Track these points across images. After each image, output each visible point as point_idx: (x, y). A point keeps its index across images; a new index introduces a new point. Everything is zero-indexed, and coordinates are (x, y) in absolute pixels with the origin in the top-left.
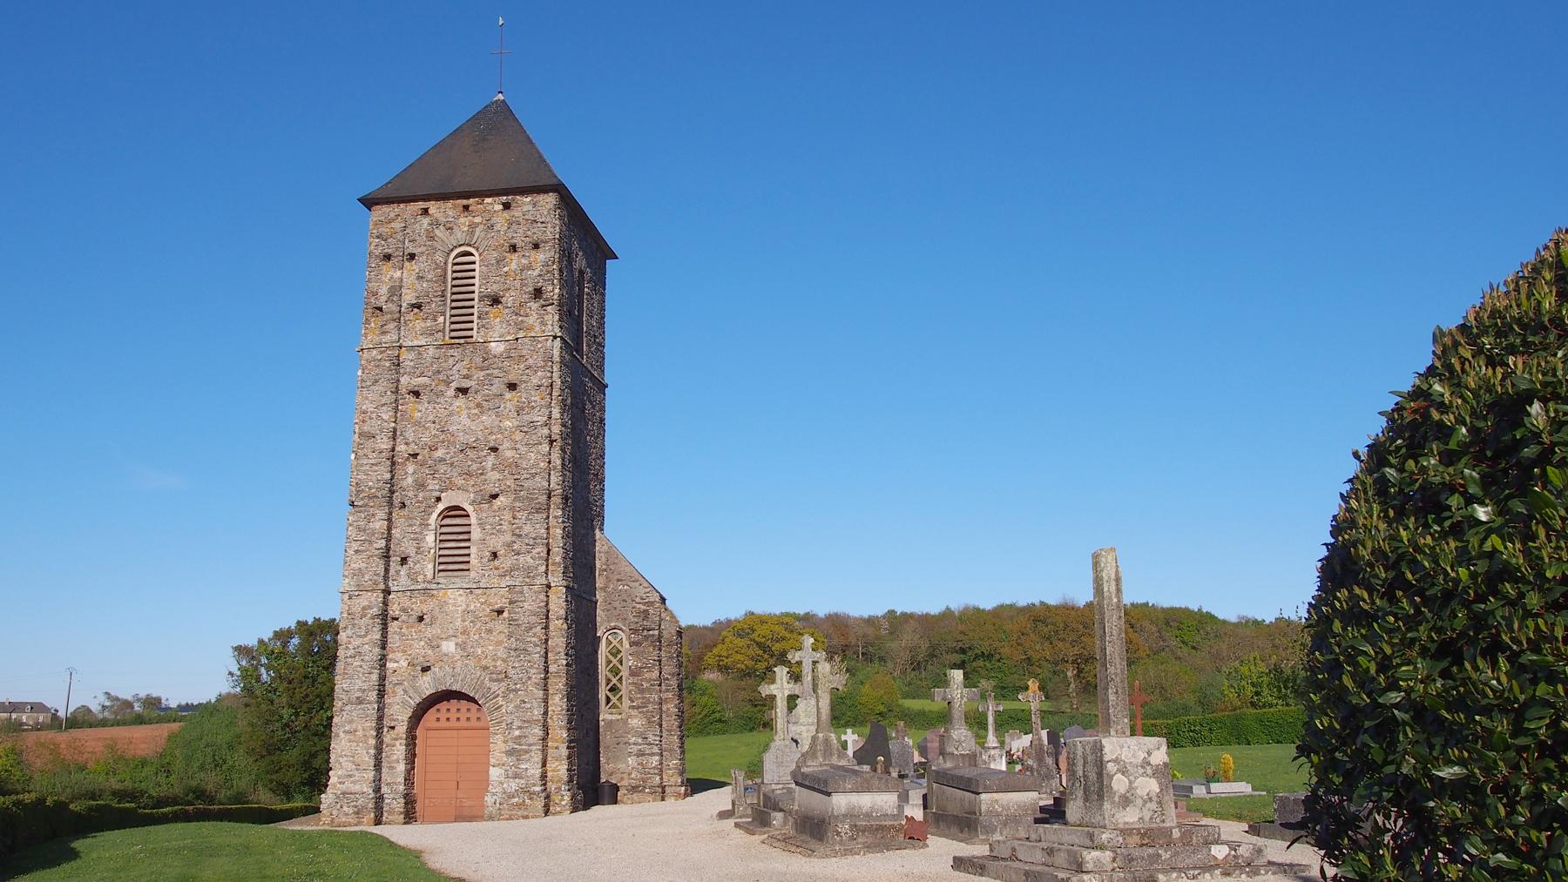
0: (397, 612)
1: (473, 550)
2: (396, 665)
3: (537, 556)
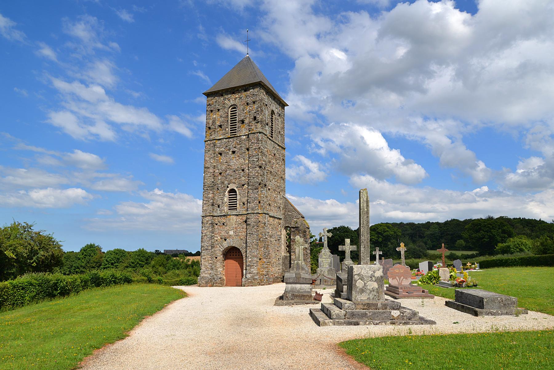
1: (238, 202)
2: (217, 238)
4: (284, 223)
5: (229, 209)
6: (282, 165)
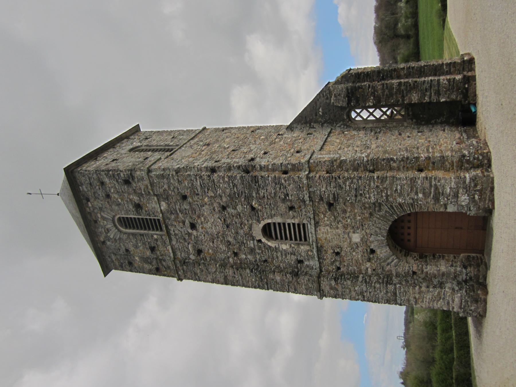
0: (334, 267)
1: (289, 221)
2: (369, 269)
3: (287, 182)
4: (341, 123)
5: (306, 240)
6: (231, 132)
